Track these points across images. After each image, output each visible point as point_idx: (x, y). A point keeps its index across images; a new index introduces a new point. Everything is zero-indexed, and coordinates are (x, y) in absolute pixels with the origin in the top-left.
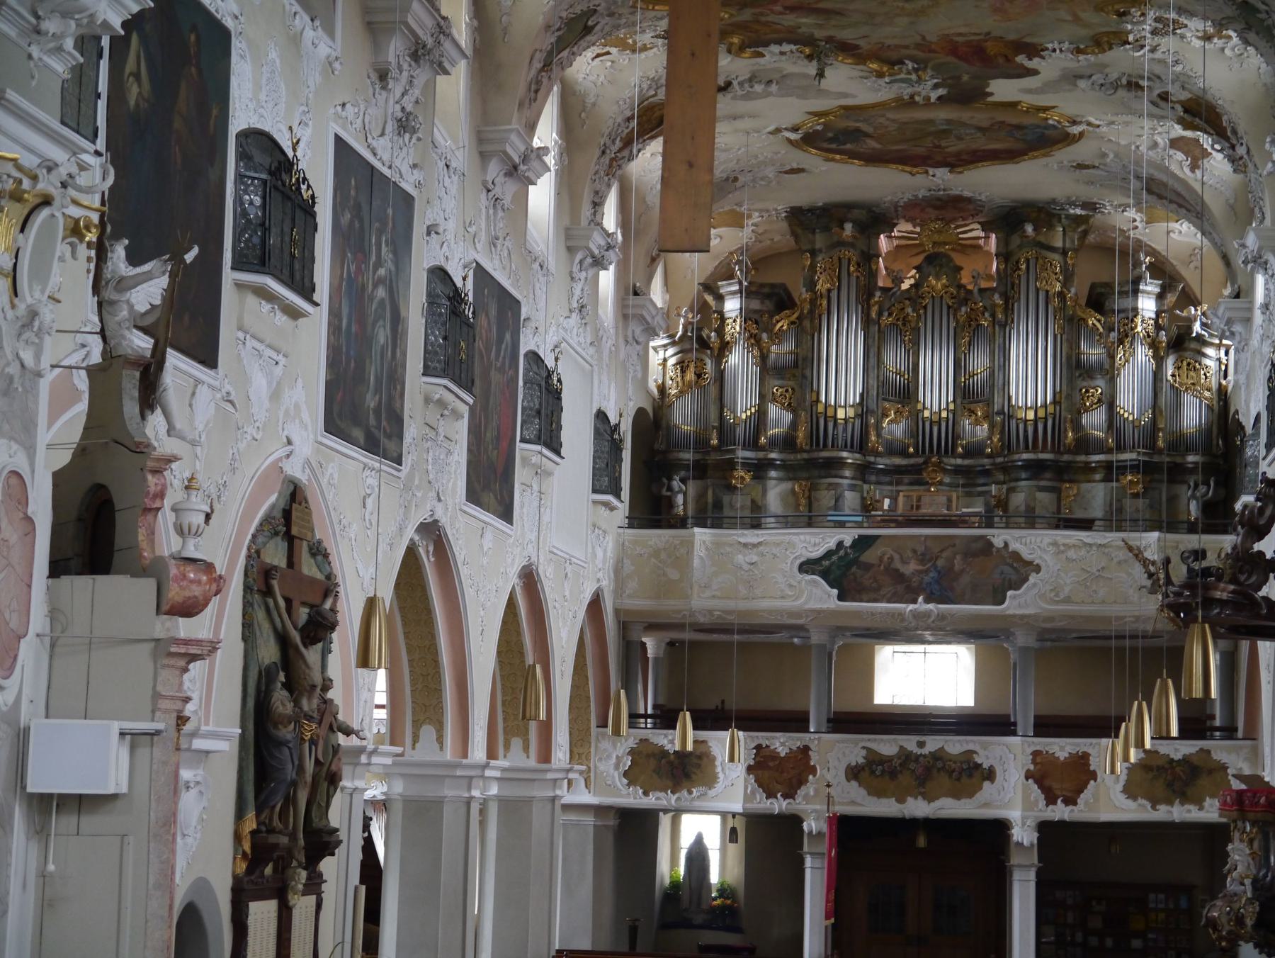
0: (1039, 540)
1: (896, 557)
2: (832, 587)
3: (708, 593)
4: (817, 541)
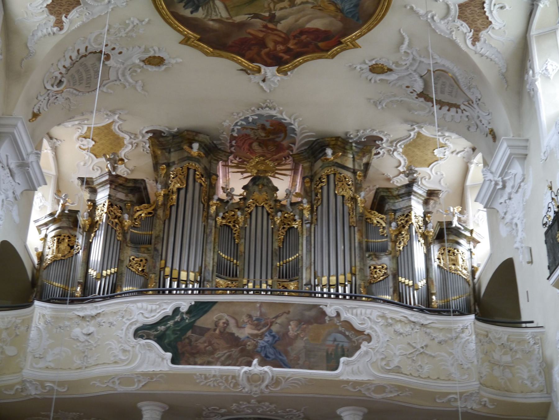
0: (368, 311)
1: (232, 322)
2: (166, 350)
3: (42, 364)
4: (154, 307)
